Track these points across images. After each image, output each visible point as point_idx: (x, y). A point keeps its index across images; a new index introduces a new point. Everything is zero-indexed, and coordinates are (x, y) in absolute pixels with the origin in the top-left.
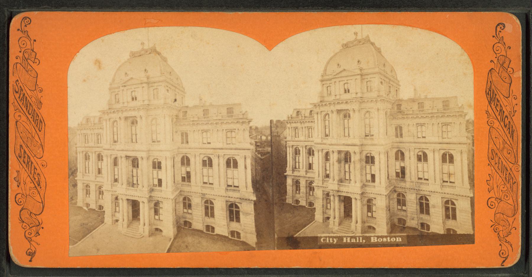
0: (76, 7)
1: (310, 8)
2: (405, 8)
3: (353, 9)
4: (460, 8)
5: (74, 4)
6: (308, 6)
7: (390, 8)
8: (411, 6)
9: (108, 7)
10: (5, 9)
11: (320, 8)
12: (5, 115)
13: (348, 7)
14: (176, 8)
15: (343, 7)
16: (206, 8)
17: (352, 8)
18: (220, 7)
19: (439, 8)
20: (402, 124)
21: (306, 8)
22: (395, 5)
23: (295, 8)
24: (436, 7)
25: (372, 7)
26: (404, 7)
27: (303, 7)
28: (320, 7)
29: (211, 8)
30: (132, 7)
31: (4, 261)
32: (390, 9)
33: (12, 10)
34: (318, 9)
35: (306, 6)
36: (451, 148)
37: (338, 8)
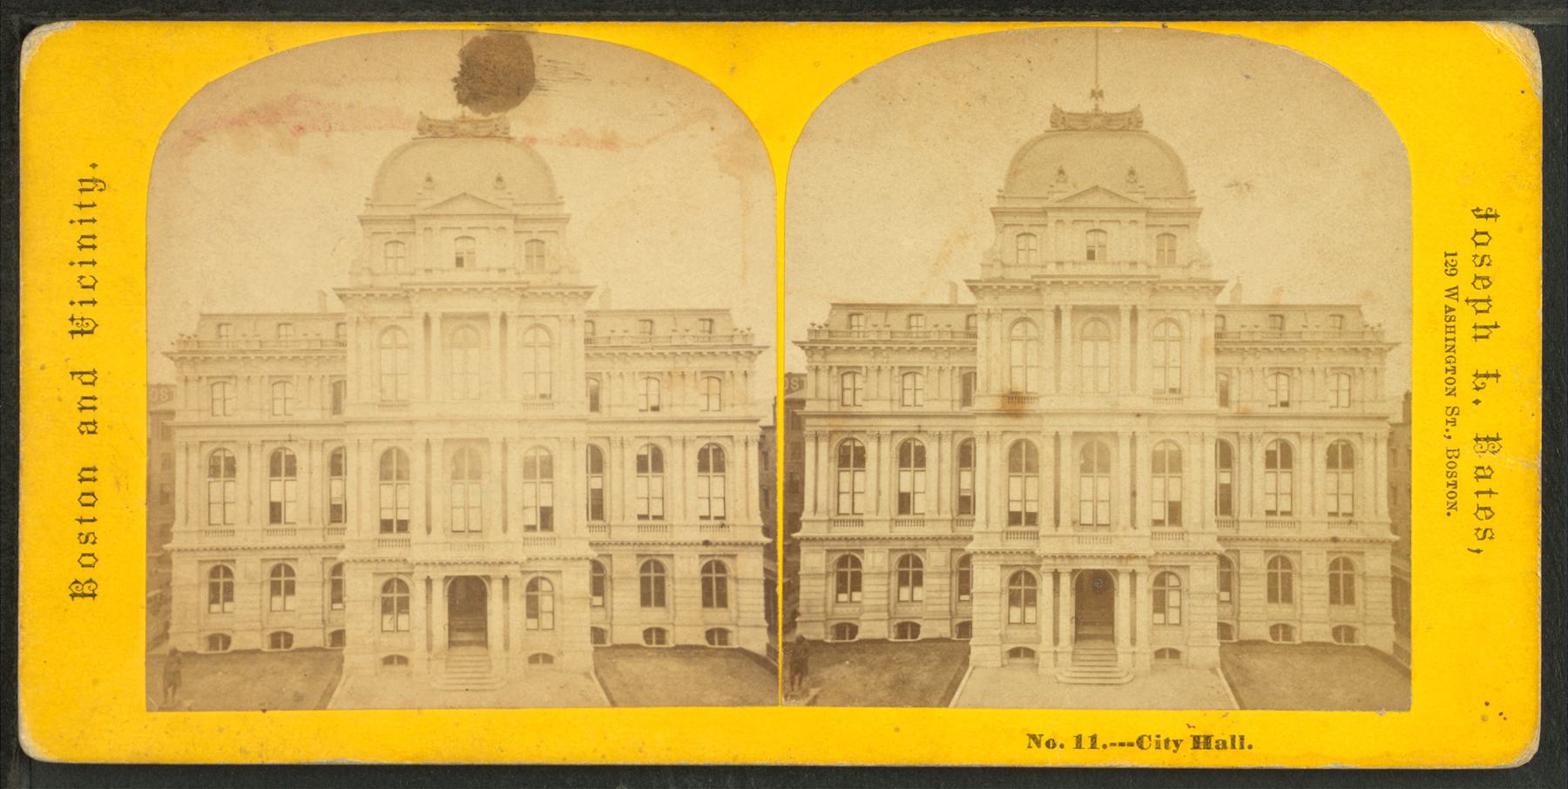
2: (1213, 12)
3: (1055, 16)
4: (1374, 12)
6: (920, 7)
8: (1230, 5)
13: (1042, 8)
15: (1026, 11)
16: (617, 13)
17: (1053, 12)
18: (656, 12)
19: (1312, 12)
21: (916, 12)
22: (1182, 4)
23: (884, 14)
24: (1306, 8)
25: (1113, 9)
26: (1208, 10)
27: (907, 11)
28: (958, 8)
29: (630, 13)
31: (13, 771)
32: (1165, 13)
35: (914, 8)
37: (1011, 13)
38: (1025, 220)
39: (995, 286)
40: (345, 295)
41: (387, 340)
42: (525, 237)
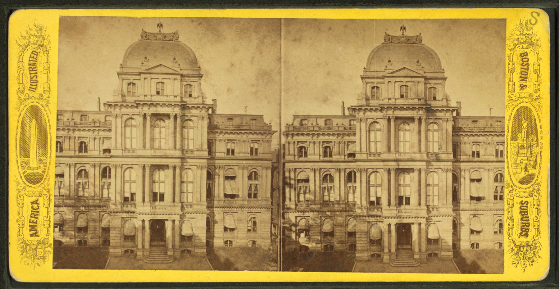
0: (79, 4)
1: (327, 4)
5: (77, 1)
6: (324, 2)
7: (412, 3)
9: (113, 4)
10: (5, 7)
11: (337, 4)
12: (5, 119)
14: (185, 5)
17: (371, 4)
18: (231, 4)
20: (212, 140)
21: (323, 4)
23: (311, 5)
25: (393, 3)
30: (139, 4)
33: (12, 8)
34: (336, 5)
35: (323, 2)
36: (378, 167)
38: (376, 81)
39: (119, 104)
40: (111, 105)
41: (129, 122)
42: (185, 83)
